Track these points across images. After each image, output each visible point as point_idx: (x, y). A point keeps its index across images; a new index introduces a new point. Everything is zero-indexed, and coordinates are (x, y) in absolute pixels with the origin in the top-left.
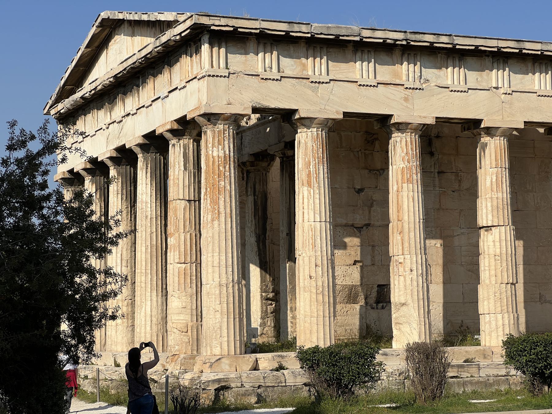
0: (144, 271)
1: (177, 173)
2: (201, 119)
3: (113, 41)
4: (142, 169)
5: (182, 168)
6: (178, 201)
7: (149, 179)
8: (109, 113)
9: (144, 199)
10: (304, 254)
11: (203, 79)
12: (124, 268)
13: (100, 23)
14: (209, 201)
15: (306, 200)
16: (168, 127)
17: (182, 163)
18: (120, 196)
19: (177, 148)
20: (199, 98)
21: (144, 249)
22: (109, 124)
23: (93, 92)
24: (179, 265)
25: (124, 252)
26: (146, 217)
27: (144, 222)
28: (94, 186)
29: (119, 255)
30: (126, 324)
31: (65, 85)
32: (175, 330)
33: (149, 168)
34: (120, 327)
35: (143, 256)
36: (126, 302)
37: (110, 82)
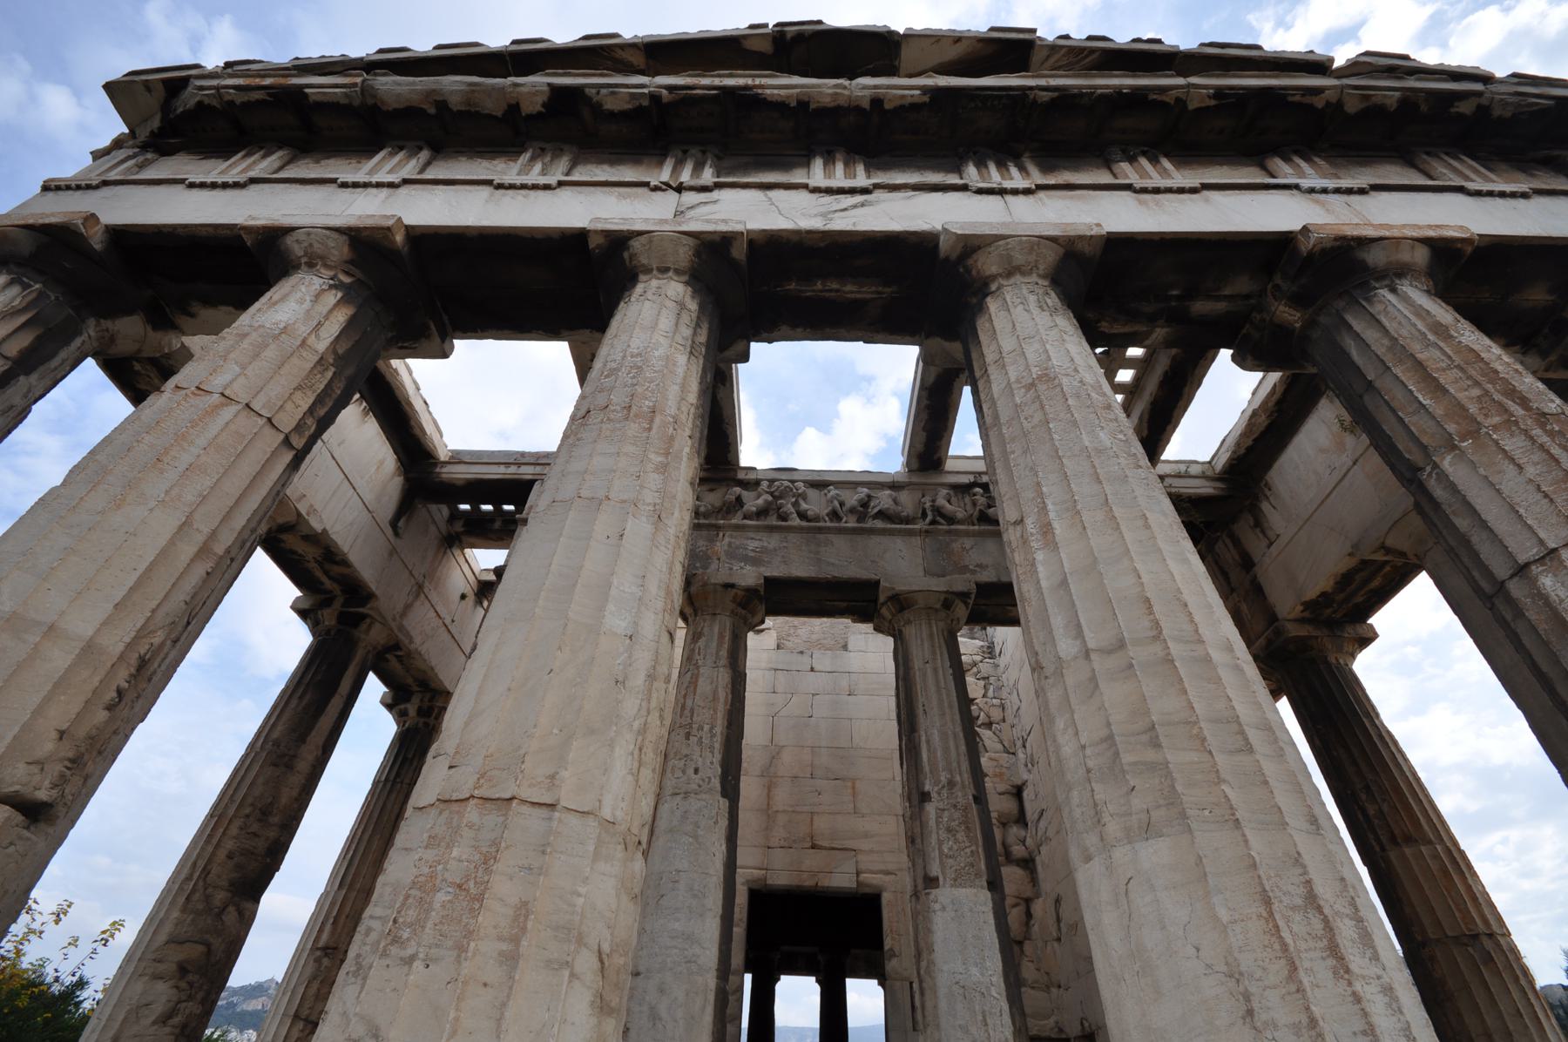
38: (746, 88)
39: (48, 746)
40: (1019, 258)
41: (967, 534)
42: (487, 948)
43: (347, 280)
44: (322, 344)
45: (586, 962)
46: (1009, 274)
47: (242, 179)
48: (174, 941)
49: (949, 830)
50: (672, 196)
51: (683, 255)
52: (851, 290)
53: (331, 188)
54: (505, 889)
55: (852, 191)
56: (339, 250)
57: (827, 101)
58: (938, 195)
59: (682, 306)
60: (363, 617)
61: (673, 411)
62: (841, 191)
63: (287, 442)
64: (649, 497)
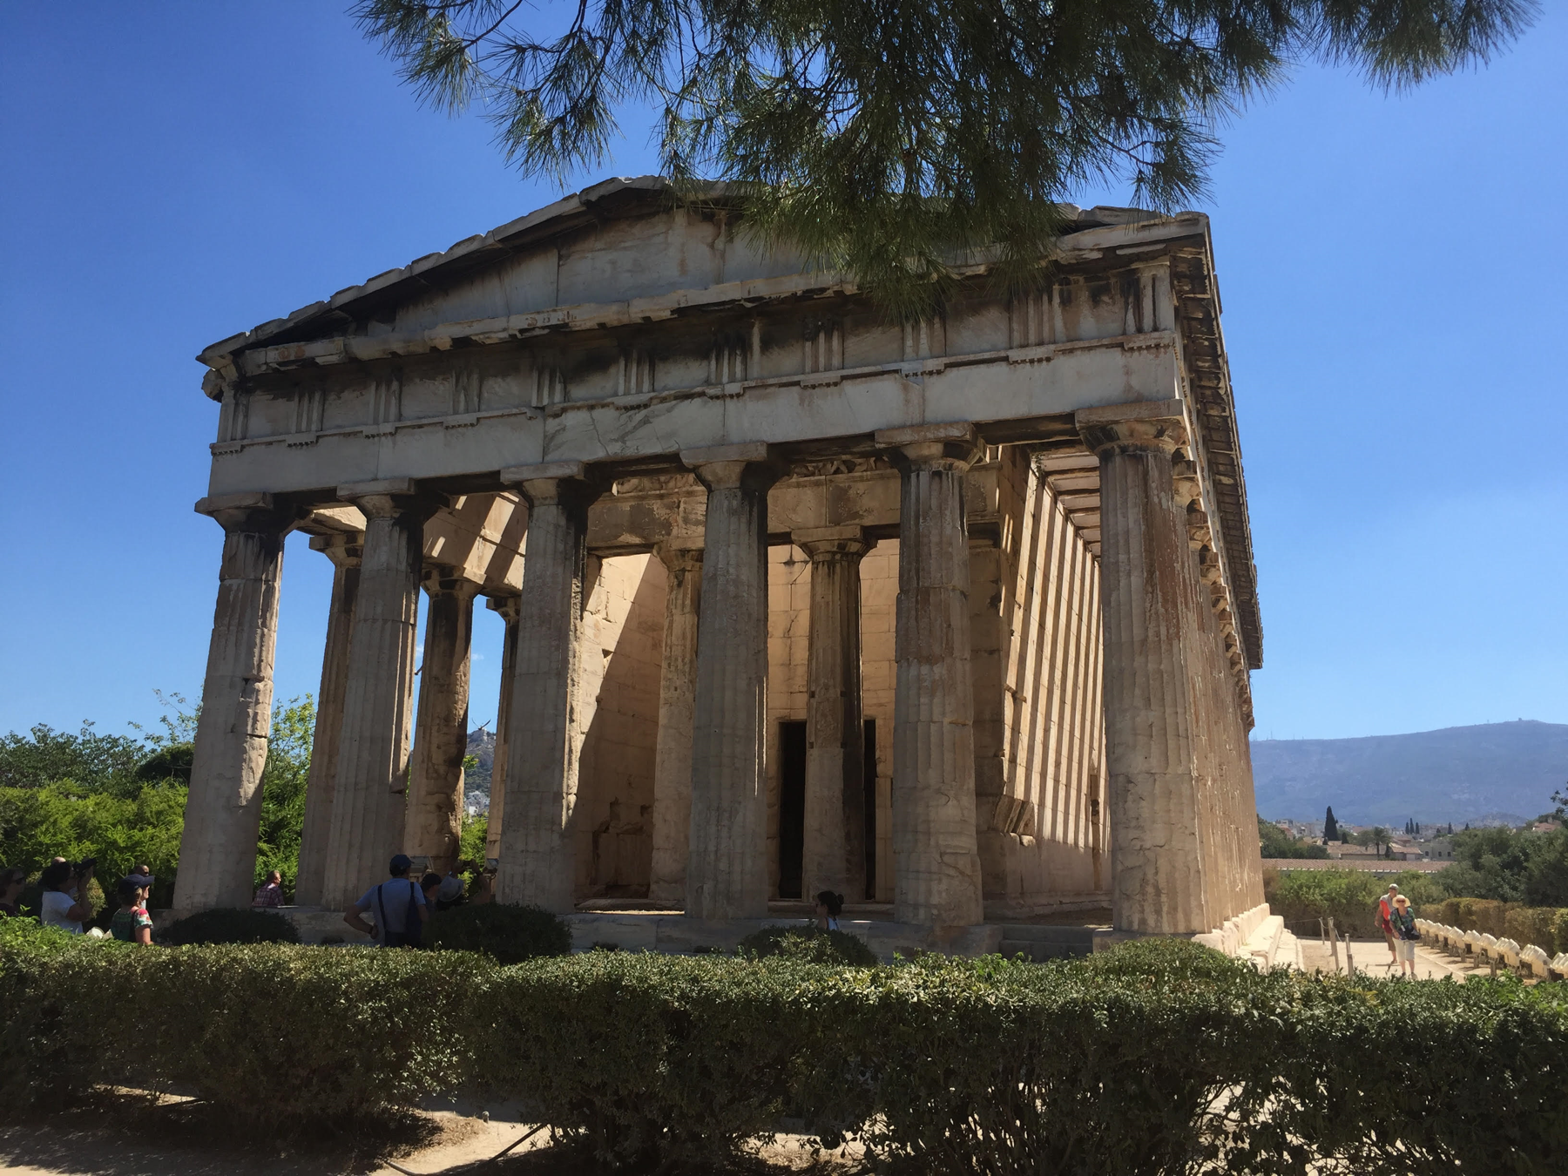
1: (948, 531)
2: (1141, 428)
3: (599, 245)
8: (558, 387)
9: (744, 578)
13: (602, 197)
16: (955, 432)
20: (1129, 388)
22: (564, 410)
23: (537, 332)
28: (405, 536)
31: (341, 308)
32: (952, 872)
37: (647, 319)
38: (566, 325)
41: (862, 479)
44: (403, 566)
47: (311, 437)
50: (537, 425)
51: (551, 489)
52: (652, 466)
55: (638, 407)
56: (387, 503)
57: (615, 323)
58: (687, 402)
59: (557, 526)
62: (632, 408)
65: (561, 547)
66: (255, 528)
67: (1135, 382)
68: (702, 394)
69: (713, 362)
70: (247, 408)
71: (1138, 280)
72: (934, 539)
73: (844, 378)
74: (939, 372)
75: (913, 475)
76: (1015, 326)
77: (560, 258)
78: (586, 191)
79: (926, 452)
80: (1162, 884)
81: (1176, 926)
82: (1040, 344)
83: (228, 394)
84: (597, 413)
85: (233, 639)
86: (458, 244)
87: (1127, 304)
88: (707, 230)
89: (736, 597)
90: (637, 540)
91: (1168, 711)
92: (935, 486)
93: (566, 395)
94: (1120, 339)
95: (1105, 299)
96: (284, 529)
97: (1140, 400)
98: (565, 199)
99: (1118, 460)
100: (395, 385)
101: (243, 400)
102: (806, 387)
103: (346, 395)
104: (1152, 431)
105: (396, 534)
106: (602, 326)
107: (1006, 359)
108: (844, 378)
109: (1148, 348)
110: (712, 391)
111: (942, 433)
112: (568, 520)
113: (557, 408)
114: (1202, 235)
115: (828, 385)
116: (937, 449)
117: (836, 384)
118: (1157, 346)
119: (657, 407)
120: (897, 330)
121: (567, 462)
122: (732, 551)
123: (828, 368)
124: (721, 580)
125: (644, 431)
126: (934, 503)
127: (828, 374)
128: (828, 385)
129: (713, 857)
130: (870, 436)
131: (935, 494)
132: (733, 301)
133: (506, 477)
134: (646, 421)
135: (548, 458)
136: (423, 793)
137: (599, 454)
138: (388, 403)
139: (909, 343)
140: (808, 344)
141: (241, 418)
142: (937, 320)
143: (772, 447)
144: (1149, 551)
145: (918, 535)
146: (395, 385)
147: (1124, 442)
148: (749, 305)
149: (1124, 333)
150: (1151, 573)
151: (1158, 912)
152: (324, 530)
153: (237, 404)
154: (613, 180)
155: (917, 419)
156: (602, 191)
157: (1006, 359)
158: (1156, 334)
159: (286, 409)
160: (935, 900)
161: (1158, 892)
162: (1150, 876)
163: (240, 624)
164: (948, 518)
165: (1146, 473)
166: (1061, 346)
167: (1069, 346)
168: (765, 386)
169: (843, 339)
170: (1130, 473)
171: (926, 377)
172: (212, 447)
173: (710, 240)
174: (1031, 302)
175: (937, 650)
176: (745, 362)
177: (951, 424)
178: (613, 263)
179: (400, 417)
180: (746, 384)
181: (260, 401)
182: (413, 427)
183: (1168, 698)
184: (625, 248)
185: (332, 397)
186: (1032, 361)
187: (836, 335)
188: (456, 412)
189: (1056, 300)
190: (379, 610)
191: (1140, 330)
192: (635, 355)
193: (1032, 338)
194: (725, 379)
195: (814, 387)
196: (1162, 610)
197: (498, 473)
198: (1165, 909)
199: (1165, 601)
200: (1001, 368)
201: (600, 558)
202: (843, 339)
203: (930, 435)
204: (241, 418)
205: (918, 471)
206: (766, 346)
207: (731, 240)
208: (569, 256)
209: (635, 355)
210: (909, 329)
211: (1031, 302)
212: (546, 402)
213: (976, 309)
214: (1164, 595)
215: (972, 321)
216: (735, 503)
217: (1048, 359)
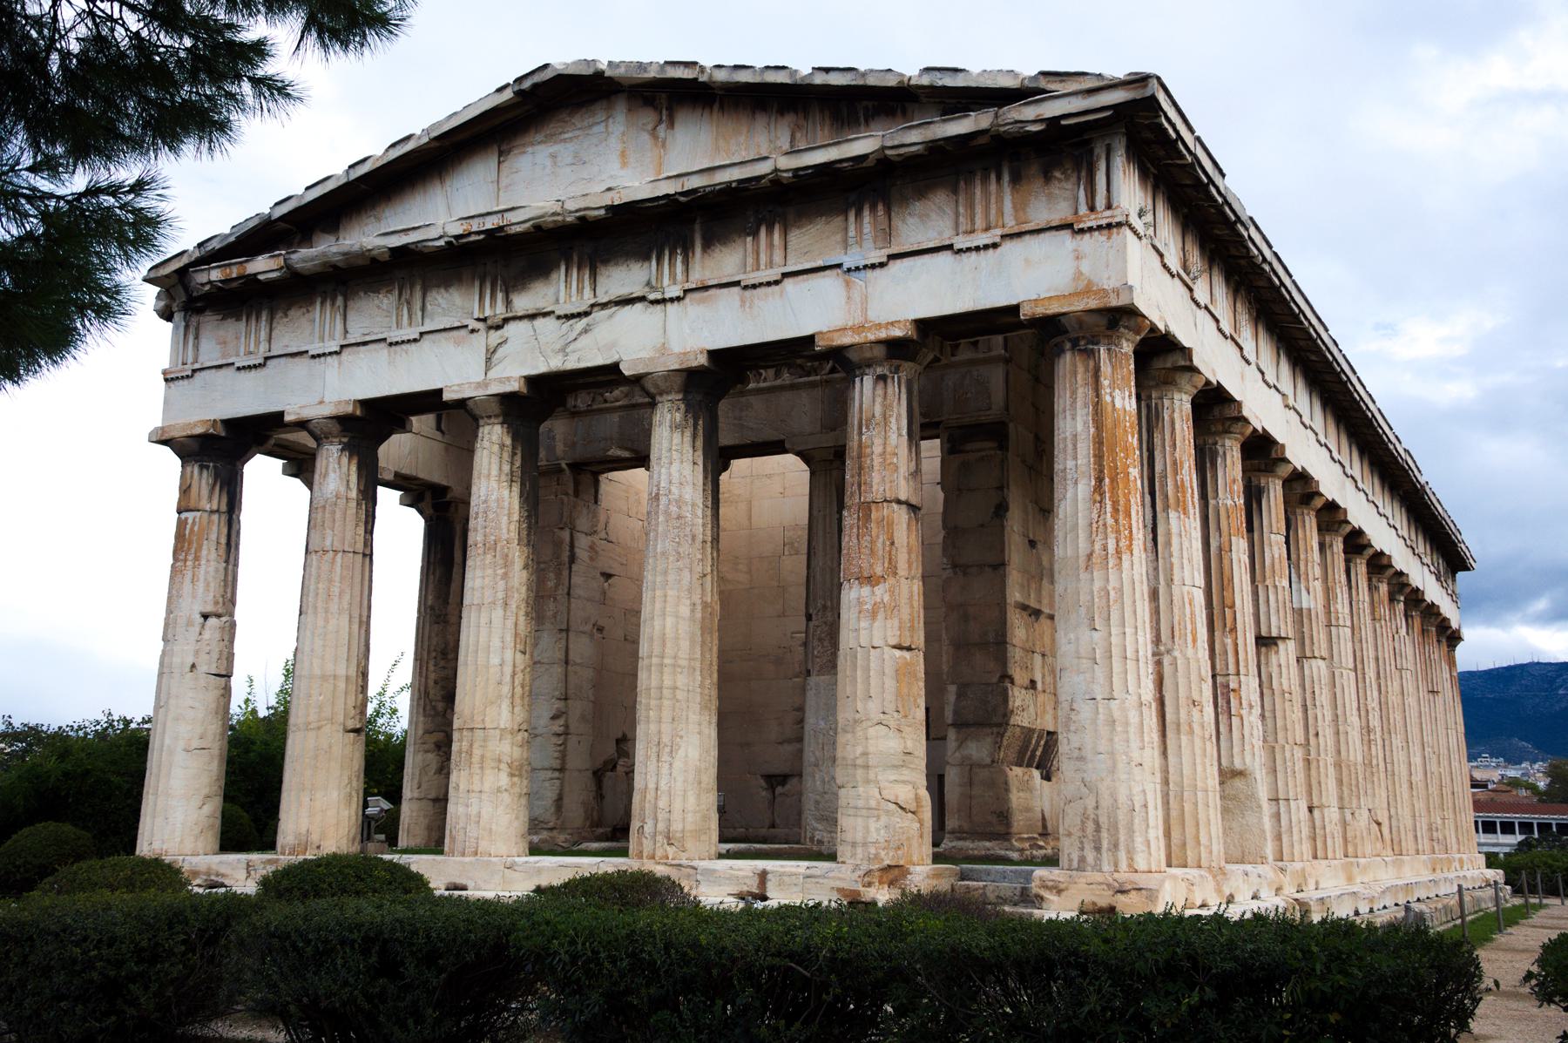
0: (683, 663)
1: (893, 438)
3: (539, 137)
4: (675, 427)
5: (904, 432)
6: (895, 506)
7: (700, 453)
8: (500, 296)
9: (688, 497)
10: (1176, 653)
11: (1105, 232)
12: (519, 655)
13: (535, 86)
14: (1109, 509)
15: (1175, 541)
16: (898, 333)
17: (904, 422)
18: (516, 489)
19: (893, 389)
20: (1081, 273)
21: (685, 610)
22: (506, 321)
23: (473, 238)
24: (898, 653)
25: (522, 619)
26: (694, 538)
27: (685, 548)
28: (355, 461)
29: (510, 623)
30: (517, 790)
31: (283, 218)
33: (700, 428)
34: (506, 795)
35: (684, 627)
36: (520, 737)
38: (501, 228)
39: (353, 712)
40: (662, 385)
42: (476, 767)
43: (345, 440)
44: (354, 494)
45: (503, 766)
46: (661, 394)
48: (427, 732)
49: (820, 640)
51: (495, 408)
52: (600, 378)
53: (304, 361)
54: (477, 752)
55: (579, 315)
56: (336, 428)
59: (502, 446)
60: (449, 503)
61: (505, 536)
62: (573, 316)
63: (364, 555)
64: (500, 595)
65: (506, 468)
66: (213, 455)
67: (1085, 267)
68: (642, 299)
69: (654, 262)
70: (197, 329)
71: (1091, 152)
72: (877, 449)
73: (785, 275)
74: (882, 265)
75: (857, 380)
76: (961, 210)
77: (501, 154)
78: (519, 80)
79: (868, 355)
80: (1103, 820)
81: (1116, 865)
82: (987, 229)
83: (178, 316)
84: (539, 322)
85: (189, 574)
86: (393, 145)
87: (1079, 179)
88: (648, 117)
89: (679, 517)
90: (626, 454)
91: (1114, 631)
92: (880, 391)
93: (508, 303)
94: (1070, 219)
95: (1058, 174)
96: (245, 456)
97: (1088, 291)
98: (500, 90)
99: (1068, 356)
100: (340, 301)
101: (194, 320)
102: (746, 287)
103: (292, 313)
104: (1103, 321)
105: (345, 460)
106: (537, 227)
107: (950, 247)
108: (785, 275)
109: (1100, 228)
110: (652, 297)
111: (883, 335)
112: (513, 440)
113: (498, 320)
114: (1153, 99)
115: (769, 284)
116: (880, 352)
117: (777, 283)
118: (1109, 226)
119: (598, 315)
120: (839, 220)
121: (508, 379)
122: (675, 468)
123: (771, 264)
124: (663, 500)
125: (584, 341)
126: (878, 410)
127: (770, 272)
128: (769, 284)
129: (653, 793)
130: (810, 339)
131: (879, 400)
132: (667, 196)
133: (447, 396)
134: (585, 331)
135: (492, 374)
136: (420, 732)
137: (541, 368)
138: (333, 319)
139: (852, 233)
140: (749, 239)
141: (191, 338)
142: (880, 207)
143: (714, 354)
144: (1099, 457)
145: (860, 445)
146: (340, 301)
147: (1073, 335)
148: (682, 199)
149: (1076, 212)
150: (1100, 480)
151: (1098, 849)
152: (293, 455)
153: (187, 327)
154: (546, 66)
155: (858, 320)
156: (537, 79)
157: (950, 247)
158: (1108, 213)
159: (233, 329)
160: (873, 837)
161: (1098, 829)
162: (1090, 811)
163: (197, 558)
164: (894, 426)
165: (1097, 370)
166: (1007, 231)
167: (1016, 230)
168: (706, 288)
169: (785, 234)
170: (1081, 369)
171: (869, 273)
172: (165, 373)
173: (650, 127)
174: (978, 182)
175: (879, 570)
176: (686, 263)
177: (892, 324)
178: (553, 156)
179: (346, 332)
180: (687, 286)
181: (209, 323)
182: (358, 344)
183: (1115, 617)
184: (565, 140)
185: (280, 314)
186: (977, 249)
187: (777, 227)
188: (399, 325)
189: (1006, 178)
190: (328, 543)
191: (1092, 208)
192: (575, 258)
193: (979, 222)
194: (666, 281)
195: (754, 286)
196: (1110, 521)
197: (439, 392)
198: (1105, 844)
199: (1116, 510)
200: (945, 258)
201: (595, 476)
202: (785, 234)
203: (871, 337)
204: (191, 338)
205: (863, 375)
206: (707, 245)
207: (671, 125)
208: (509, 151)
209: (575, 258)
210: (852, 218)
211: (978, 182)
212: (488, 313)
213: (922, 193)
214: (1115, 504)
215: (918, 206)
216: (678, 416)
217: (995, 246)
